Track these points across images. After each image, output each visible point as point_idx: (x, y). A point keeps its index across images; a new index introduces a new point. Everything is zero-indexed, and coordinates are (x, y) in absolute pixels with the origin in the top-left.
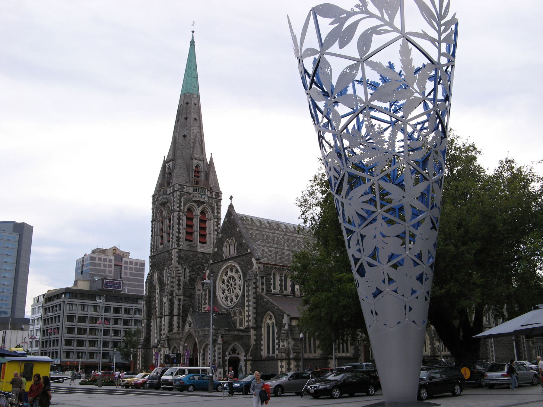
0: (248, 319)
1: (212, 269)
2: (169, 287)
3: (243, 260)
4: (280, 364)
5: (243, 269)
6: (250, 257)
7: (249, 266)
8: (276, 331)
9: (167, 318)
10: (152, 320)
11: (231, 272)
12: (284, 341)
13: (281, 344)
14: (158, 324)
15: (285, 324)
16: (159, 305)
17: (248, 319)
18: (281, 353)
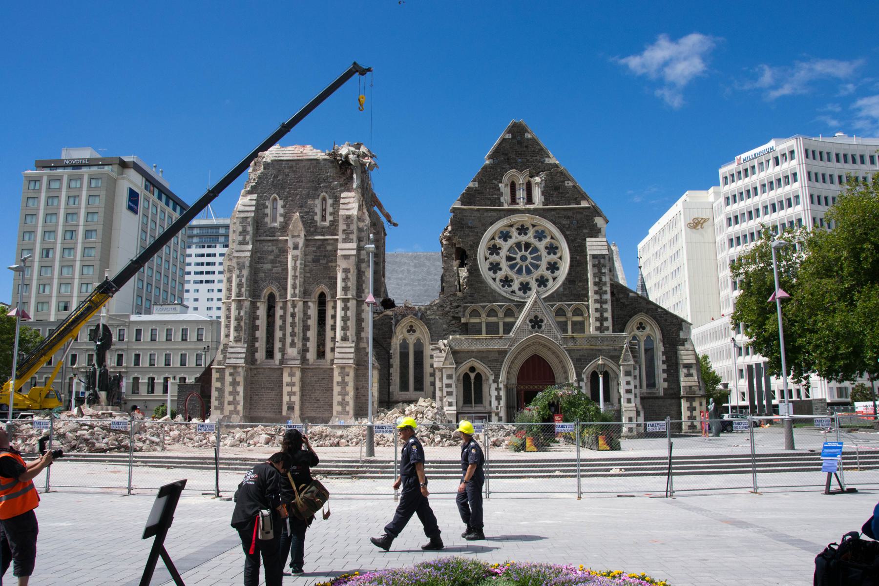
0: (602, 324)
1: (461, 219)
2: (354, 237)
3: (568, 218)
4: (684, 405)
5: (568, 233)
6: (587, 216)
7: (585, 231)
8: (659, 348)
9: (352, 304)
10: (259, 304)
11: (520, 234)
12: (692, 367)
13: (683, 372)
14: (299, 315)
16: (301, 273)
17: (602, 324)
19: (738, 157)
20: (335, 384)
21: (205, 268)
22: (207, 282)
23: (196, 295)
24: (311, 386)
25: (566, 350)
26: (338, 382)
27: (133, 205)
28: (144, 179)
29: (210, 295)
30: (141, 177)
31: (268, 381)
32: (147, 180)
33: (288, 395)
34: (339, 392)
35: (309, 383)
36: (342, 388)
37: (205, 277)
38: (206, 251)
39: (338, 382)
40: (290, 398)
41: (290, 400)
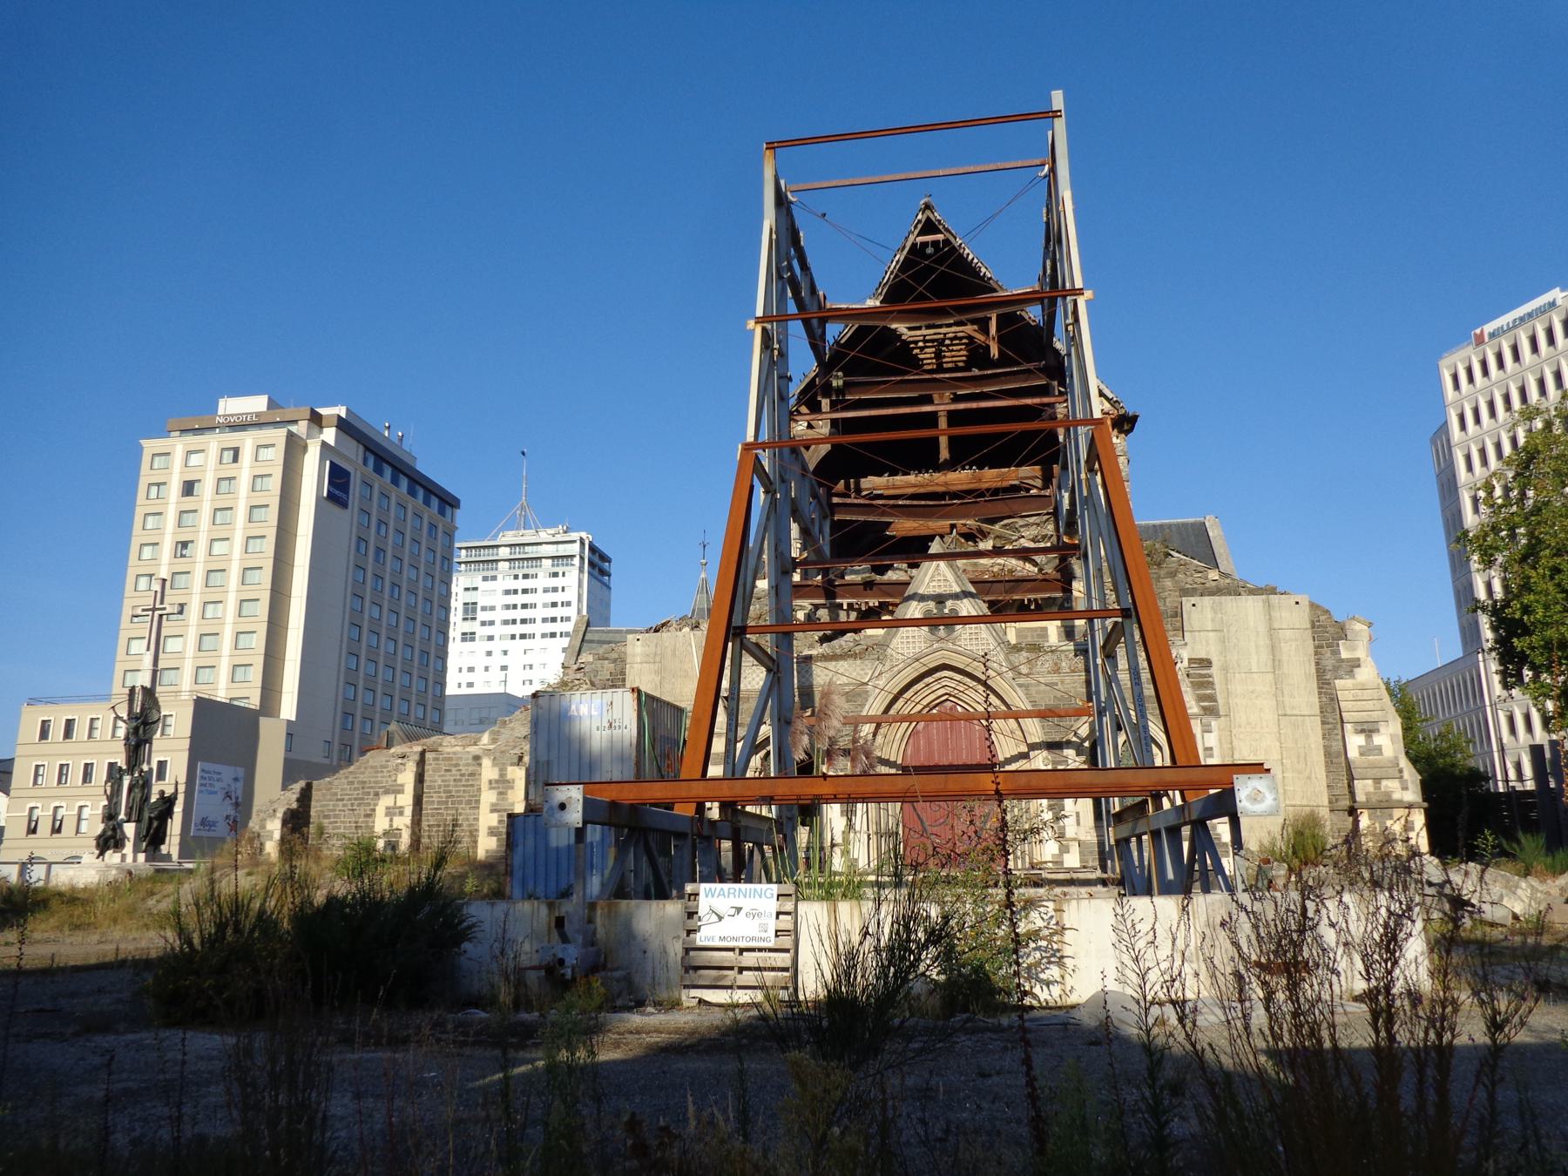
12: (1378, 731)
15: (1355, 664)
18: (1377, 781)
19: (1478, 331)
20: (484, 786)
21: (519, 614)
22: (523, 636)
23: (504, 661)
24: (445, 792)
25: (1020, 686)
26: (490, 782)
27: (337, 492)
28: (361, 448)
29: (528, 660)
30: (354, 443)
31: (352, 783)
32: (367, 449)
33: (386, 815)
34: (493, 805)
35: (440, 786)
36: (500, 793)
37: (519, 629)
38: (521, 584)
39: (490, 782)
40: (391, 820)
41: (391, 826)
